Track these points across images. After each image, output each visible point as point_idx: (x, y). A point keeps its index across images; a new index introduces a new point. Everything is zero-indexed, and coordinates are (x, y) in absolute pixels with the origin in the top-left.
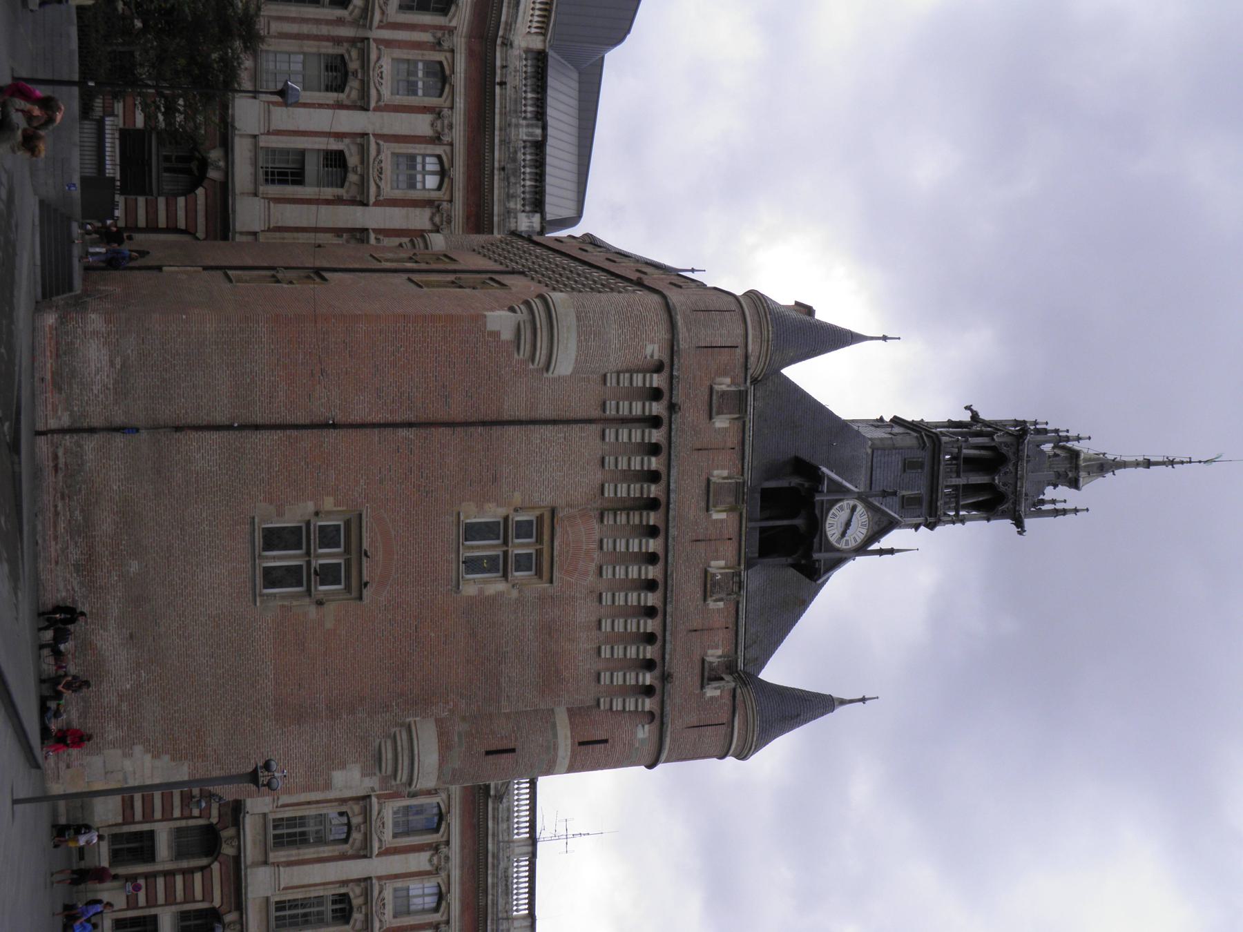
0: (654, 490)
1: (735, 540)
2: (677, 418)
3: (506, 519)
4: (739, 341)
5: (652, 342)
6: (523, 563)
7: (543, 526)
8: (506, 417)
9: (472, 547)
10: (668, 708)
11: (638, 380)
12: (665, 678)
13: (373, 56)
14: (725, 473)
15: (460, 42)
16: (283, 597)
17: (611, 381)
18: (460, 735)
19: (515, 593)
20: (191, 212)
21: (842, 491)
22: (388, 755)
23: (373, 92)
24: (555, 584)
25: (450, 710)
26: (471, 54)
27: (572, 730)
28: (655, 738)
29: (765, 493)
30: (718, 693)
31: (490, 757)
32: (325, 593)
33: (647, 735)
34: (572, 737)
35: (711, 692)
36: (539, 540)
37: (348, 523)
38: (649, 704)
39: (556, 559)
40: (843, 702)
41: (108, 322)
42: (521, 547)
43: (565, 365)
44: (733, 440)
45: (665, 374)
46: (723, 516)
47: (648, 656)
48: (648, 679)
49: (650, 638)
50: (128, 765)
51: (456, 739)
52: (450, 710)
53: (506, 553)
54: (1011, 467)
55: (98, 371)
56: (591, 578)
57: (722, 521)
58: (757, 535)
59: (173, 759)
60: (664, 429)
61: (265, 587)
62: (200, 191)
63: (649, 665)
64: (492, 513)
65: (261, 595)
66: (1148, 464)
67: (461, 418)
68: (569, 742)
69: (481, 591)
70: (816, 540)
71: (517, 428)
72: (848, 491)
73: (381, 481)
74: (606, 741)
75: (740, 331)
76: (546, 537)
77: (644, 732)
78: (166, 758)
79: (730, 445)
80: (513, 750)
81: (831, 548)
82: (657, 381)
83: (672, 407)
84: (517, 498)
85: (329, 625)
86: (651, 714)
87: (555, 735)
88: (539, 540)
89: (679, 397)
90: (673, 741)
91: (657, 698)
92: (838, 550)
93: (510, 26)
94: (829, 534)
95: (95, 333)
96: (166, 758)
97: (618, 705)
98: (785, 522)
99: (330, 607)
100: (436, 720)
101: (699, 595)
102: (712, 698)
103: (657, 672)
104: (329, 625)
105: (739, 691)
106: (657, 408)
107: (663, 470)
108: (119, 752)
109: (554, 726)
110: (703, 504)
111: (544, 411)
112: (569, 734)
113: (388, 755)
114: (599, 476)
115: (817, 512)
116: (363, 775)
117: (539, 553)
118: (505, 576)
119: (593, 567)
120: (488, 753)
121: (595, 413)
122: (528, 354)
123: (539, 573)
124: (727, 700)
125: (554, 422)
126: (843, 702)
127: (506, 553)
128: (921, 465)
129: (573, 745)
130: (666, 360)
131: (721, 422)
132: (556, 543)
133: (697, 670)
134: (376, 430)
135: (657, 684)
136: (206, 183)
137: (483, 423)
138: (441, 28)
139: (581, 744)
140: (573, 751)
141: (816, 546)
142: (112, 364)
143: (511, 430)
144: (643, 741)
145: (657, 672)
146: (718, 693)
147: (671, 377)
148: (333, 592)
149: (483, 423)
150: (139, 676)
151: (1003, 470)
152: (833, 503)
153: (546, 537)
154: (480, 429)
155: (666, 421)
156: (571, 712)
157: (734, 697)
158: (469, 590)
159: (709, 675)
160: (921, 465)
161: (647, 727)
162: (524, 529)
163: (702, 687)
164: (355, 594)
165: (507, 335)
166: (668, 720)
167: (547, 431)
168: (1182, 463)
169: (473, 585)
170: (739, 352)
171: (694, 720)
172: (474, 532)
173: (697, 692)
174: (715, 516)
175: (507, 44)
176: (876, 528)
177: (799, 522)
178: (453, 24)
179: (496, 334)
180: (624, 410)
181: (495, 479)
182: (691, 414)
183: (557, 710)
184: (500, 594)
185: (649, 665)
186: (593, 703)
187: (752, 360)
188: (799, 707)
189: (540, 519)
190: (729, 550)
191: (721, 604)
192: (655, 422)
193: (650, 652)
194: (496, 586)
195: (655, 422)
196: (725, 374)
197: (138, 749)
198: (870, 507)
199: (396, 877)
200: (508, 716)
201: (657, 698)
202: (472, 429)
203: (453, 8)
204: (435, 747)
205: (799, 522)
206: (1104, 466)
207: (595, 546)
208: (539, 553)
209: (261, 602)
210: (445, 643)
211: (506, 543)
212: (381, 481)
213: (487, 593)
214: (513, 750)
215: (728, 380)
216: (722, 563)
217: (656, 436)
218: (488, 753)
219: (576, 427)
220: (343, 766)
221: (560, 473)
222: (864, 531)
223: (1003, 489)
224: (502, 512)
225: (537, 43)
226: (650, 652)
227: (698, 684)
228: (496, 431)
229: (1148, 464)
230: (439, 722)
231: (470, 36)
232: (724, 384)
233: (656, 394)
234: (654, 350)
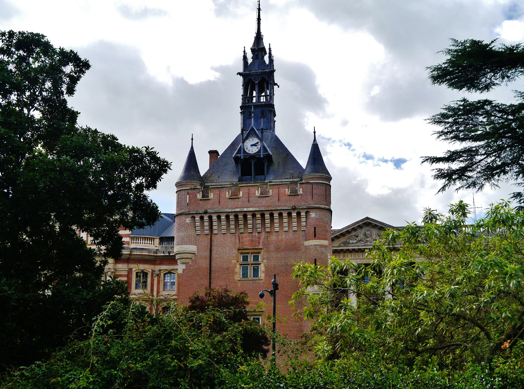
0: (232, 217)
1: (249, 188)
2: (209, 211)
3: (241, 265)
4: (186, 192)
5: (186, 220)
6: (256, 258)
7: (243, 252)
11: (198, 224)
12: (294, 209)
13: (162, 297)
15: (157, 268)
17: (199, 232)
19: (265, 261)
23: (174, 297)
26: (161, 264)
28: (313, 210)
29: (243, 175)
30: (301, 189)
33: (314, 214)
35: (300, 192)
36: (248, 253)
38: (303, 214)
40: (315, 140)
42: (251, 259)
43: (193, 248)
44: (217, 191)
45: (195, 216)
46: (241, 193)
47: (286, 215)
48: (294, 214)
49: (280, 215)
53: (252, 264)
54: (253, 78)
57: (243, 193)
58: (257, 177)
60: (213, 215)
63: (290, 214)
64: (238, 269)
66: (259, 19)
67: (208, 280)
69: (263, 272)
71: (212, 262)
72: (241, 146)
75: (183, 192)
76: (247, 251)
77: (313, 215)
79: (218, 192)
80: (315, 260)
81: (259, 151)
82: (197, 218)
83: (206, 212)
84: (234, 261)
86: (307, 213)
87: (311, 245)
88: (248, 253)
90: (317, 204)
91: (301, 211)
93: (149, 250)
97: (304, 224)
98: (253, 167)
102: (303, 191)
103: (292, 211)
106: (206, 218)
110: (237, 200)
111: (208, 254)
114: (228, 235)
121: (209, 237)
122: (190, 260)
123: (259, 253)
124: (304, 186)
125: (211, 250)
126: (315, 140)
129: (315, 239)
130: (191, 215)
131: (211, 196)
133: (293, 197)
135: (296, 211)
137: (210, 273)
138: (152, 274)
139: (315, 237)
143: (213, 264)
144: (316, 215)
145: (292, 211)
147: (196, 214)
149: (210, 273)
152: (245, 152)
153: (247, 251)
154: (212, 274)
155: (210, 214)
156: (306, 240)
159: (294, 193)
162: (245, 259)
164: (261, 313)
165: (184, 267)
167: (214, 252)
168: (259, 5)
169: (262, 275)
171: (310, 197)
172: (245, 275)
174: (241, 195)
175: (156, 251)
176: (254, 135)
178: (151, 271)
179: (184, 270)
180: (207, 228)
181: (228, 269)
183: (305, 245)
185: (290, 214)
186: (304, 232)
187: (193, 187)
188: (316, 155)
189: (241, 253)
190: (252, 189)
192: (210, 218)
193: (285, 214)
194: (262, 268)
195: (210, 218)
196: (196, 196)
198: (247, 138)
201: (301, 211)
202: (212, 277)
203: (145, 271)
206: (259, 38)
207: (251, 234)
208: (252, 253)
211: (249, 264)
215: (198, 195)
217: (214, 218)
219: (213, 243)
221: (227, 248)
224: (238, 266)
225: (157, 241)
226: (285, 214)
227: (297, 197)
228: (213, 269)
229: (259, 19)
231: (155, 264)
232: (199, 196)
233: (202, 218)
234: (188, 220)
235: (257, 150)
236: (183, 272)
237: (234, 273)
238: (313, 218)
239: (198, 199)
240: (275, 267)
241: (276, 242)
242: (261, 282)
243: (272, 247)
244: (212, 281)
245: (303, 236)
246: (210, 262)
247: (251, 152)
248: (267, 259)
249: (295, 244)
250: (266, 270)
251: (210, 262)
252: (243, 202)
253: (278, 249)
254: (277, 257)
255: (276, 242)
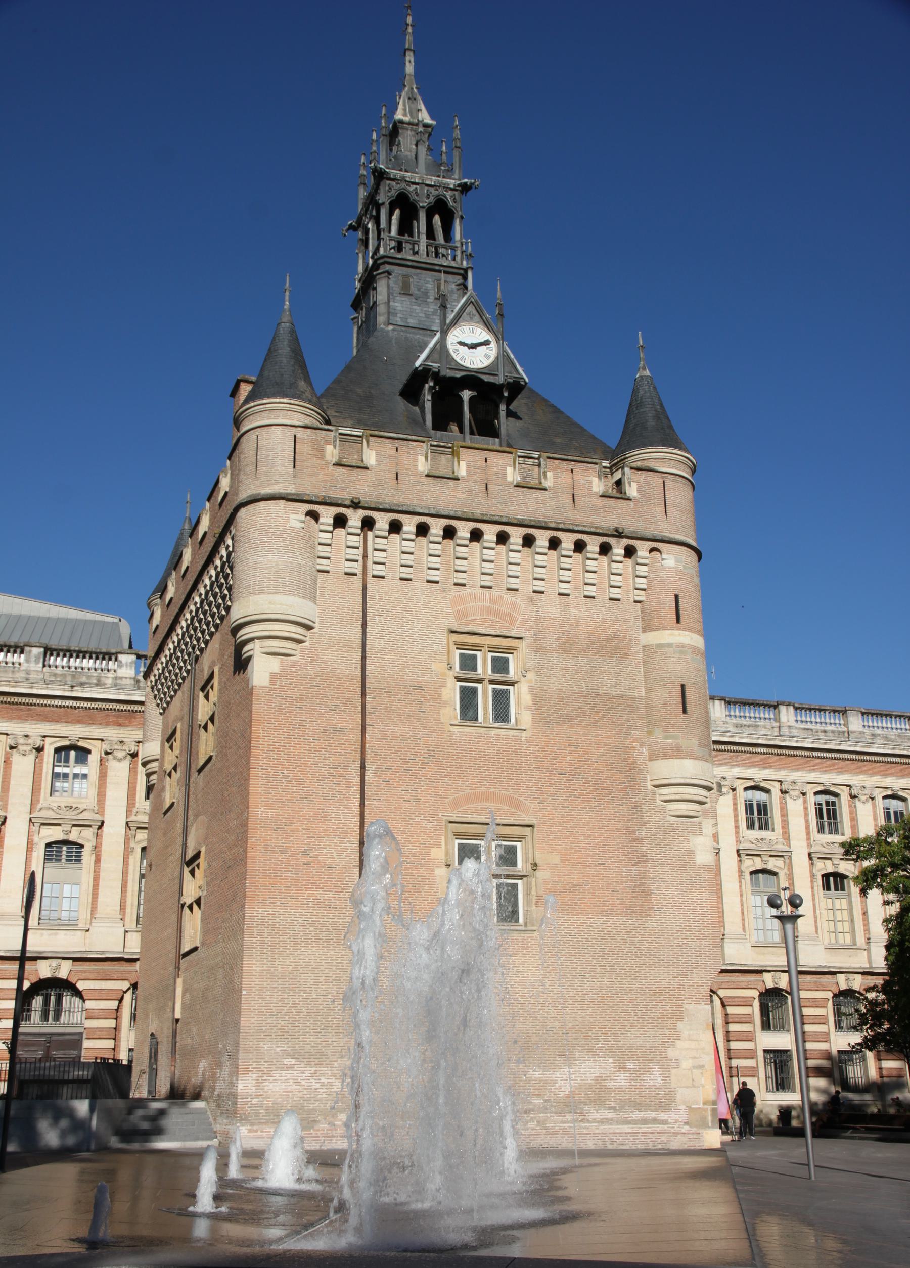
2: (365, 500)
4: (290, 432)
5: (287, 520)
6: (501, 665)
8: (358, 672)
9: (485, 714)
10: (648, 534)
12: (619, 534)
14: (421, 459)
16: (528, 902)
18: (666, 738)
19: (530, 675)
20: (102, 995)
21: (441, 350)
22: (683, 808)
24: (522, 635)
25: (641, 746)
27: (665, 629)
29: (436, 427)
30: (634, 485)
31: (688, 708)
32: (525, 861)
34: (672, 629)
35: (632, 490)
36: (478, 647)
37: (458, 836)
39: (498, 633)
41: (247, 1071)
46: (463, 464)
50: (686, 1064)
51: (670, 741)
52: (641, 746)
55: (297, 1083)
56: (518, 599)
57: (468, 466)
59: (681, 1019)
61: (517, 921)
62: (81, 986)
64: (452, 692)
65: (526, 924)
68: (676, 632)
69: (528, 708)
70: (486, 378)
73: (418, 800)
74: (677, 597)
78: (680, 1025)
80: (683, 686)
84: (439, 667)
85: (556, 859)
87: (669, 645)
88: (478, 647)
89: (346, 496)
92: (497, 358)
94: (480, 366)
95: (258, 1084)
96: (680, 1025)
99: (539, 858)
100: (650, 760)
101: (539, 494)
102: (639, 491)
103: (612, 541)
104: (556, 859)
105: (633, 465)
107: (418, 519)
108: (673, 1071)
109: (660, 646)
112: (669, 632)
113: (683, 808)
115: (458, 375)
116: (701, 834)
117: (492, 649)
118: (512, 684)
119: (508, 597)
120: (685, 711)
121: (357, 582)
123: (511, 650)
125: (364, 625)
127: (492, 682)
128: (406, 277)
129: (679, 629)
132: (483, 632)
134: (366, 803)
136: (73, 980)
137: (364, 694)
139: (678, 621)
140: (685, 629)
141: (491, 379)
142: (291, 1067)
144: (678, 561)
146: (634, 485)
148: (525, 853)
149: (364, 694)
150: (600, 1049)
151: (413, 197)
157: (638, 469)
158: (526, 719)
160: (406, 277)
161: (664, 556)
162: (468, 663)
163: (629, 499)
165: (275, 664)
166: (659, 534)
170: (300, 433)
173: (632, 504)
177: (466, 395)
179: (274, 678)
181: (419, 688)
182: (360, 486)
184: (531, 689)
191: (549, 474)
196: (322, 451)
197: (671, 1053)
199: (737, 827)
200: (649, 690)
202: (368, 707)
204: (677, 762)
205: (466, 395)
208: (492, 649)
209: (533, 925)
210: (577, 747)
212: (418, 800)
213: (530, 703)
214: (683, 686)
216: (509, 470)
218: (685, 711)
220: (691, 853)
222: (479, 330)
223: (432, 199)
227: (624, 502)
230: (652, 757)
235: (486, 363)
236: (273, 682)
237: (437, 700)
238: (670, 570)
239: (327, 463)
240: (560, 699)
241: (562, 625)
242: (524, 734)
243: (551, 640)
244: (368, 721)
245: (636, 618)
246: (364, 658)
247: (467, 364)
248: (539, 671)
249: (616, 637)
250: (535, 702)
251: (364, 658)
252: (470, 491)
253: (567, 646)
254: (567, 669)
255: (562, 625)
